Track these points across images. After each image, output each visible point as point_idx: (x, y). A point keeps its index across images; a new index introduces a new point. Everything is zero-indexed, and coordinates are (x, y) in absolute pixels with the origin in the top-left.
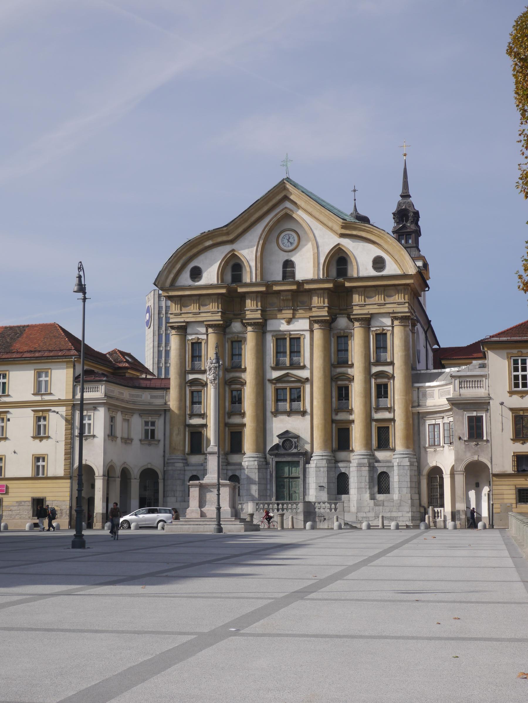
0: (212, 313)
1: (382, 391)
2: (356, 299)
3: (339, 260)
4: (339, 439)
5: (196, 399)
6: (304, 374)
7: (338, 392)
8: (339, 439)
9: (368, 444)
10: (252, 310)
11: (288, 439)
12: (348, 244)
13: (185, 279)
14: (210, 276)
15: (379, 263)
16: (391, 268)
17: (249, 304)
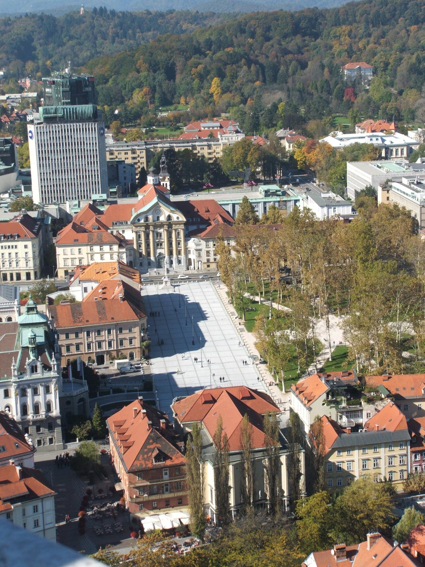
0: (143, 229)
1: (179, 244)
2: (173, 225)
3: (169, 217)
4: (171, 253)
5: (140, 246)
6: (163, 240)
7: (170, 244)
8: (171, 253)
9: (177, 255)
10: (151, 228)
11: (160, 254)
12: (171, 214)
13: (136, 221)
14: (142, 221)
15: (178, 218)
16: (180, 219)
17: (151, 227)
